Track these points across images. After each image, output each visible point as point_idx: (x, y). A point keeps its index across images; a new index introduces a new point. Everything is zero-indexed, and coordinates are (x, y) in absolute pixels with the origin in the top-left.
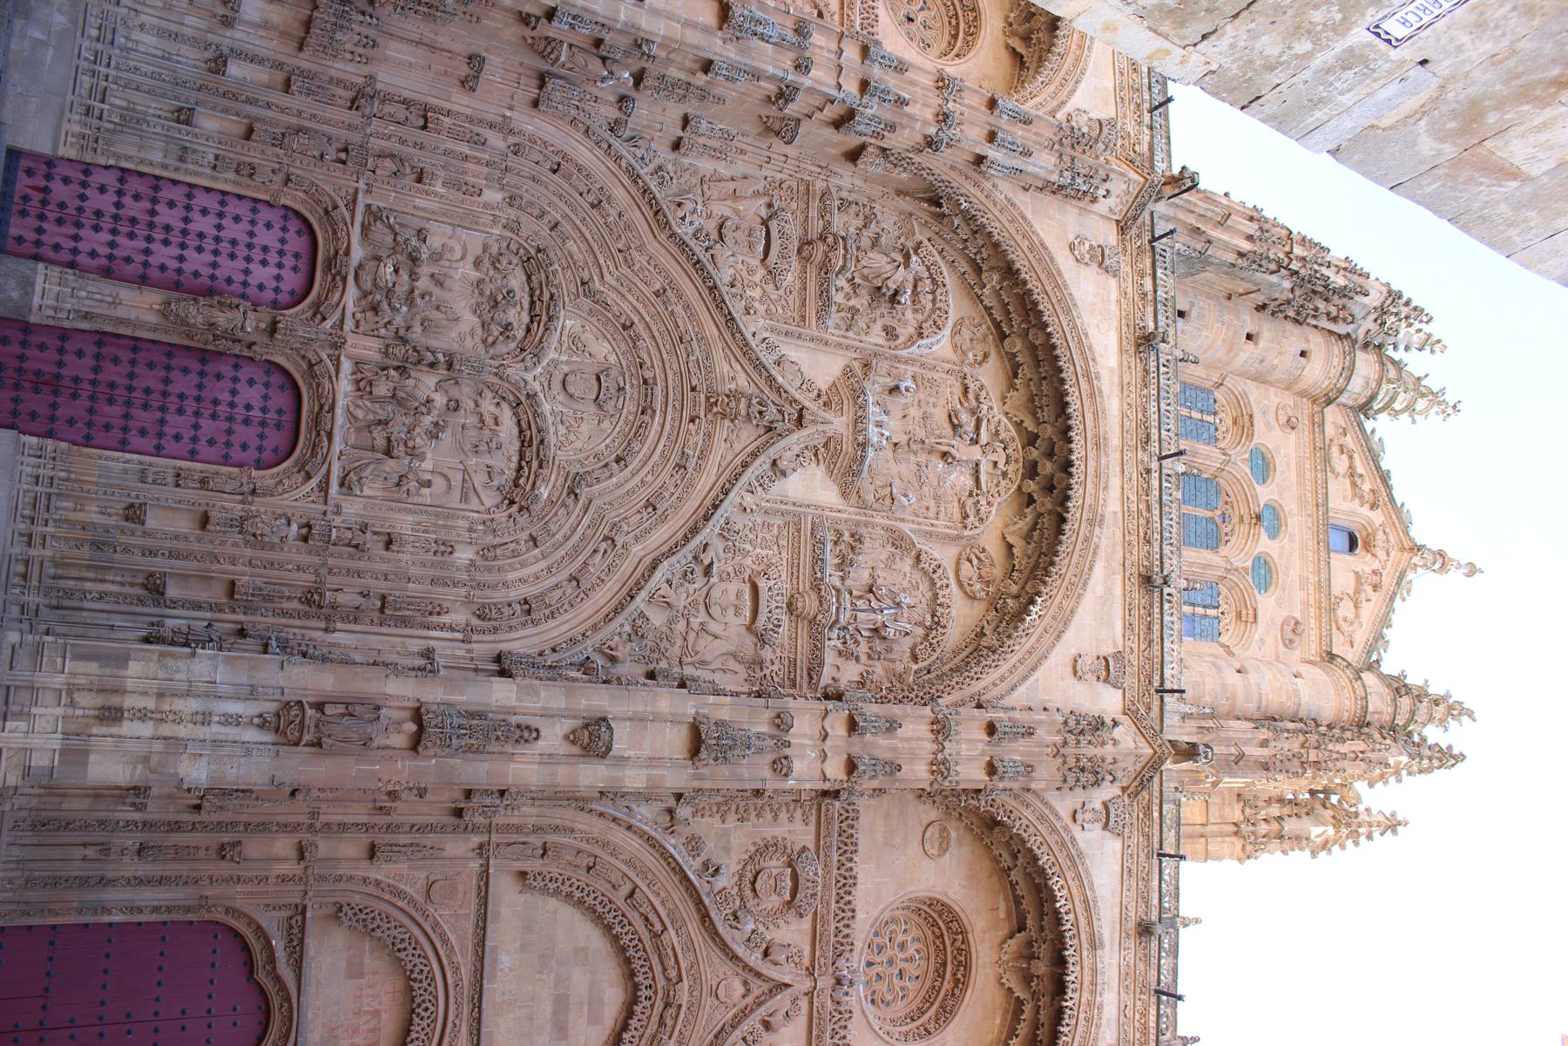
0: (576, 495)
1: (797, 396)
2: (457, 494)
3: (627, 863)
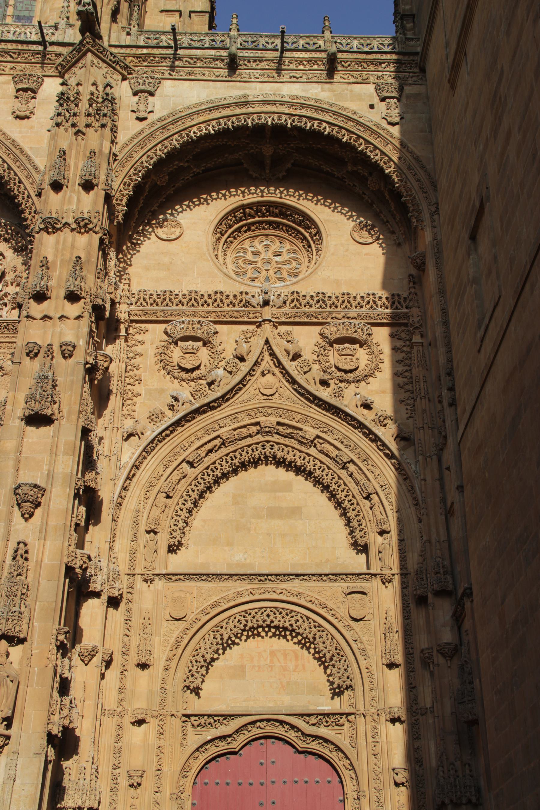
3: (166, 467)
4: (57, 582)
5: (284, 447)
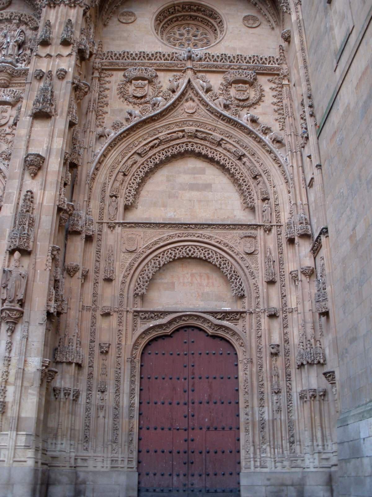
4: (51, 218)
5: (200, 146)
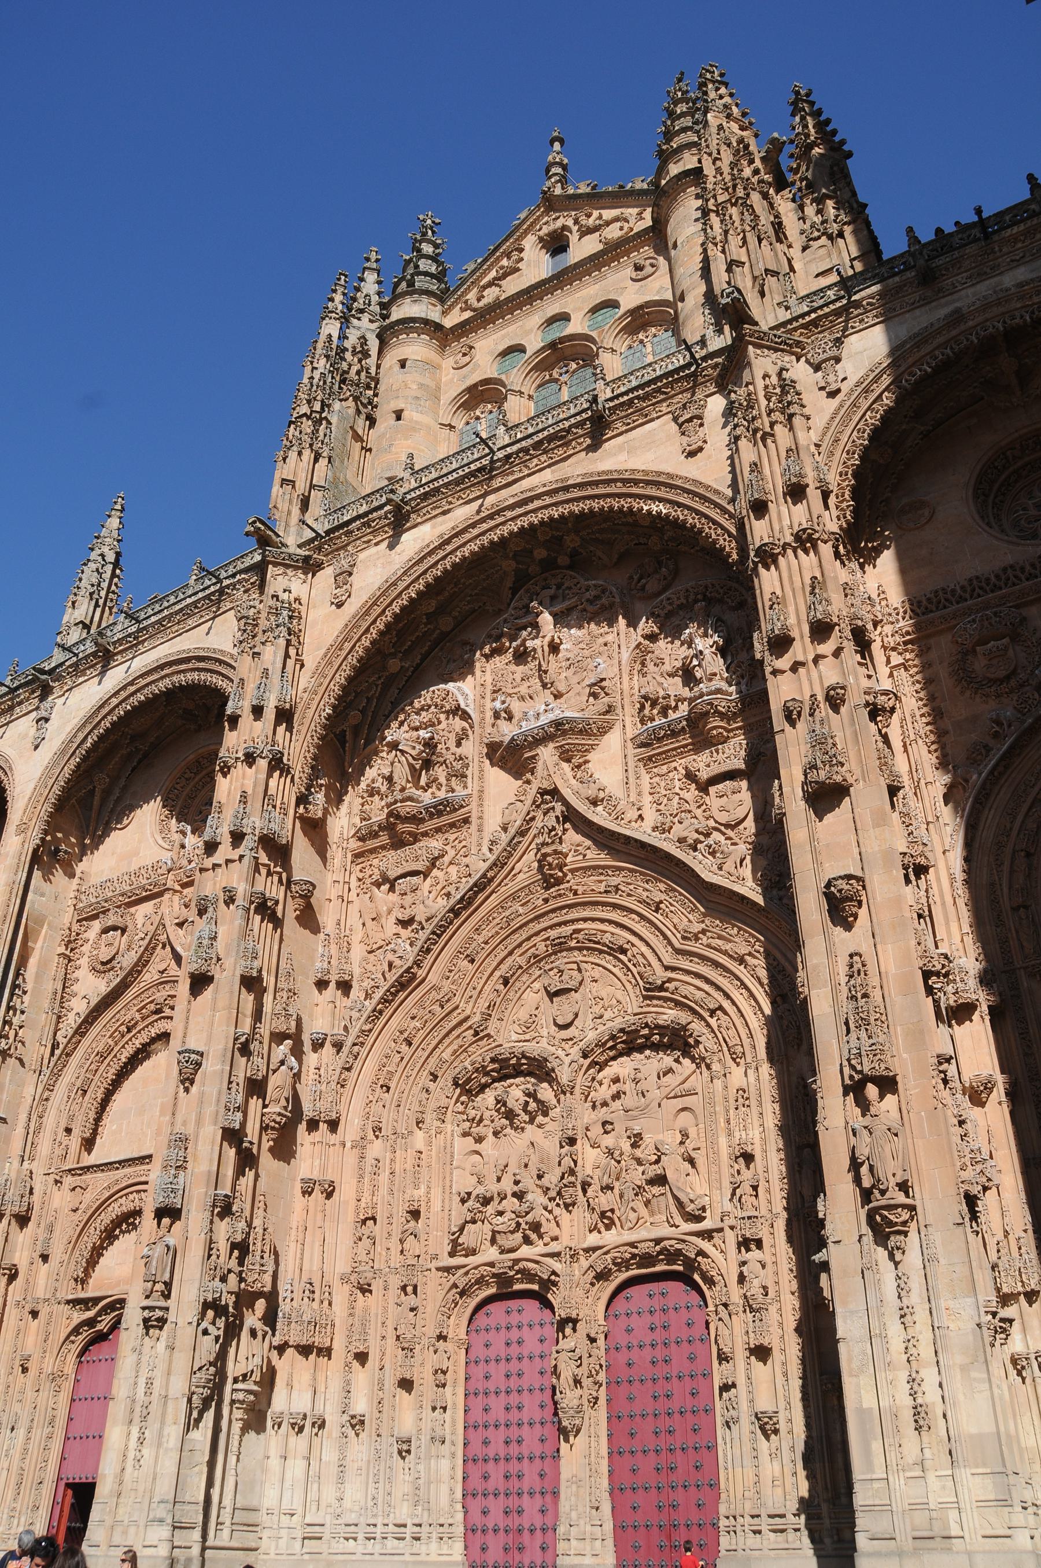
0: (664, 983)
1: (529, 802)
2: (687, 1101)
